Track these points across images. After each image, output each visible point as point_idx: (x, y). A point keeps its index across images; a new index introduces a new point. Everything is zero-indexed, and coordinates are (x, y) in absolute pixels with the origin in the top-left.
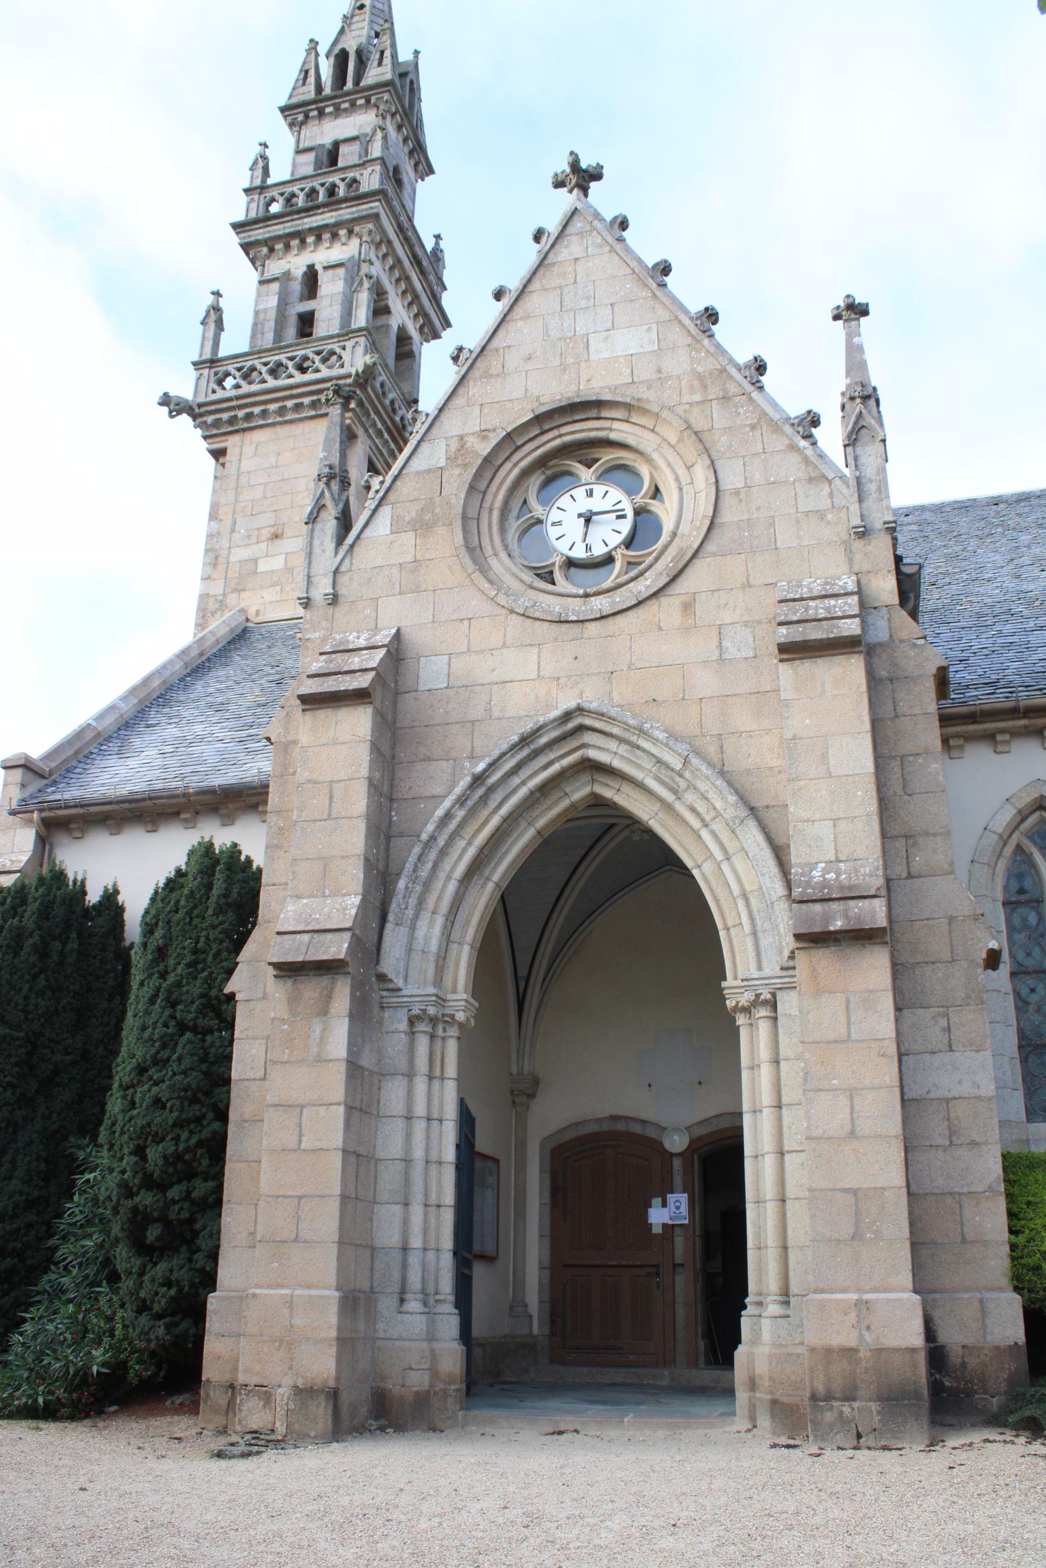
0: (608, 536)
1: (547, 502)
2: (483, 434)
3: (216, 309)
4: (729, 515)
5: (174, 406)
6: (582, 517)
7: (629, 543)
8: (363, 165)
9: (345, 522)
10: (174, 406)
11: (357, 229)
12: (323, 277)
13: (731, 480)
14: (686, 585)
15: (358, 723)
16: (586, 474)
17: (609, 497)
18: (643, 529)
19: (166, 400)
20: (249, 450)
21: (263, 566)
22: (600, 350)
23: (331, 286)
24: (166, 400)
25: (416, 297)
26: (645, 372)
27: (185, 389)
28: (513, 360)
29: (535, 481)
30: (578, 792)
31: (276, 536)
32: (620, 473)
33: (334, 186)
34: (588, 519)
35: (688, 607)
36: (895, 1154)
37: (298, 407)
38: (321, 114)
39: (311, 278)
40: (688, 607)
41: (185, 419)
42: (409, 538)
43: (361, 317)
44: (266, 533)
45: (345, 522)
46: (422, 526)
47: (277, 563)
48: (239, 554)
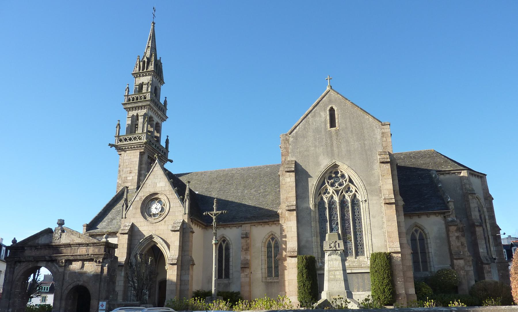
2: (143, 196)
3: (119, 125)
6: (155, 208)
7: (160, 212)
9: (127, 206)
12: (140, 118)
17: (159, 206)
18: (162, 210)
19: (110, 145)
21: (128, 178)
22: (158, 185)
23: (141, 120)
24: (110, 145)
25: (160, 116)
28: (148, 185)
31: (130, 173)
32: (160, 202)
37: (134, 147)
38: (140, 76)
39: (137, 116)
41: (114, 148)
44: (129, 172)
45: (127, 206)
46: (136, 208)
47: (131, 178)
48: (124, 176)
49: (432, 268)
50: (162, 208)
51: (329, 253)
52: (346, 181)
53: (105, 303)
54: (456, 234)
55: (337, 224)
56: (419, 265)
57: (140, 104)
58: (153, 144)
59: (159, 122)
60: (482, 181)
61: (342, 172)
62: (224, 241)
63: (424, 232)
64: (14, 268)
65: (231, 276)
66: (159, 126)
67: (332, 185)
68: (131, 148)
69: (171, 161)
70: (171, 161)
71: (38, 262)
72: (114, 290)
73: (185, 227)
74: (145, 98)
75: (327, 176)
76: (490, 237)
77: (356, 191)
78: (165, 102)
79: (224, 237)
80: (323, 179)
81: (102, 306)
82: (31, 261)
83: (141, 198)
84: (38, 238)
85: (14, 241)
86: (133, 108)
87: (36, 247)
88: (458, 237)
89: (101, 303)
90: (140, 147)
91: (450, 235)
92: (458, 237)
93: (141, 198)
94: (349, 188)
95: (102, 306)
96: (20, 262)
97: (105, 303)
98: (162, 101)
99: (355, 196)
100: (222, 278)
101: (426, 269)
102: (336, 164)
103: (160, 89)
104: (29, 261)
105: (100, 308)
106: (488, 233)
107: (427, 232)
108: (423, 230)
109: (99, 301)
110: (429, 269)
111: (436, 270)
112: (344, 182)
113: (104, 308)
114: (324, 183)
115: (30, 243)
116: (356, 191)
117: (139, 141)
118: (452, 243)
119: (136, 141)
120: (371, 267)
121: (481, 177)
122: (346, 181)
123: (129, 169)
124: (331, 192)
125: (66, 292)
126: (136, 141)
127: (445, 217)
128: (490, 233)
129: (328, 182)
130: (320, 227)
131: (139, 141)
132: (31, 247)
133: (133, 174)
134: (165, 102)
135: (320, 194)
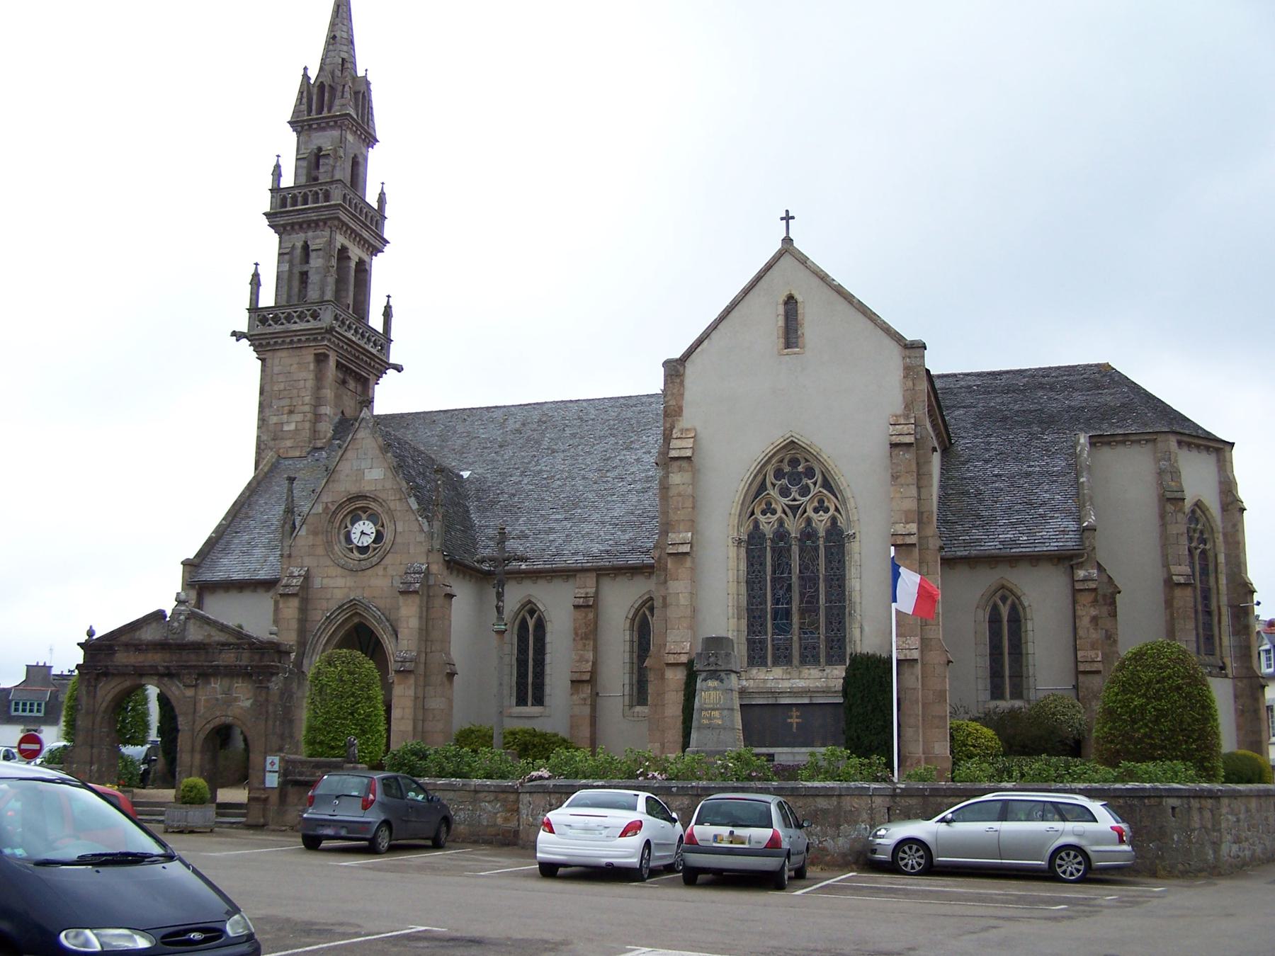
0: (367, 541)
1: (353, 524)
4: (399, 540)
5: (237, 335)
6: (363, 532)
7: (374, 542)
8: (332, 182)
10: (237, 335)
11: (329, 223)
12: (313, 255)
13: (399, 529)
14: (386, 561)
15: (295, 603)
16: (364, 516)
17: (369, 527)
18: (379, 537)
19: (234, 334)
20: (276, 361)
23: (316, 262)
24: (234, 334)
26: (379, 487)
27: (244, 328)
29: (349, 519)
30: (356, 620)
31: (291, 412)
33: (317, 193)
34: (362, 533)
35: (385, 569)
36: (411, 723)
40: (385, 569)
42: (311, 537)
43: (329, 295)
45: (294, 527)
47: (292, 427)
48: (274, 420)
49: (1032, 691)
50: (377, 531)
51: (704, 675)
52: (815, 484)
53: (276, 759)
54: (1093, 612)
55: (789, 588)
56: (1003, 683)
57: (313, 216)
58: (350, 327)
59: (366, 258)
60: (1218, 460)
61: (807, 461)
62: (532, 612)
63: (1021, 603)
64: (95, 687)
65: (547, 700)
66: (366, 270)
67: (785, 492)
68: (292, 342)
69: (399, 369)
70: (399, 369)
71: (141, 675)
72: (292, 737)
73: (431, 582)
74: (327, 197)
75: (770, 469)
76: (1224, 610)
77: (837, 509)
78: (382, 199)
79: (530, 602)
80: (760, 478)
81: (273, 764)
82: (130, 674)
83: (327, 507)
84: (140, 629)
85: (91, 633)
86: (292, 225)
87: (139, 647)
88: (1095, 620)
89: (269, 759)
90: (315, 340)
91: (1079, 613)
92: (1095, 620)
93: (327, 507)
94: (821, 502)
95: (273, 764)
96: (106, 674)
97: (276, 759)
98: (372, 199)
99: (834, 519)
100: (526, 705)
101: (1017, 693)
102: (792, 442)
103: (366, 159)
104: (123, 675)
105: (269, 767)
106: (1218, 601)
107: (1026, 604)
108: (1018, 598)
109: (265, 754)
110: (1025, 692)
111: (1041, 695)
112: (812, 486)
113: (276, 768)
114: (762, 488)
115: (124, 639)
116: (837, 509)
117: (313, 324)
118: (1081, 632)
119: (303, 326)
120: (845, 692)
121: (1218, 450)
122: (815, 484)
123: (286, 402)
124: (779, 510)
125: (202, 736)
126: (303, 326)
127: (1072, 567)
128: (1224, 600)
129: (774, 485)
130: (749, 595)
131: (313, 324)
132: (127, 646)
133: (298, 417)
134: (382, 199)
135: (753, 513)
